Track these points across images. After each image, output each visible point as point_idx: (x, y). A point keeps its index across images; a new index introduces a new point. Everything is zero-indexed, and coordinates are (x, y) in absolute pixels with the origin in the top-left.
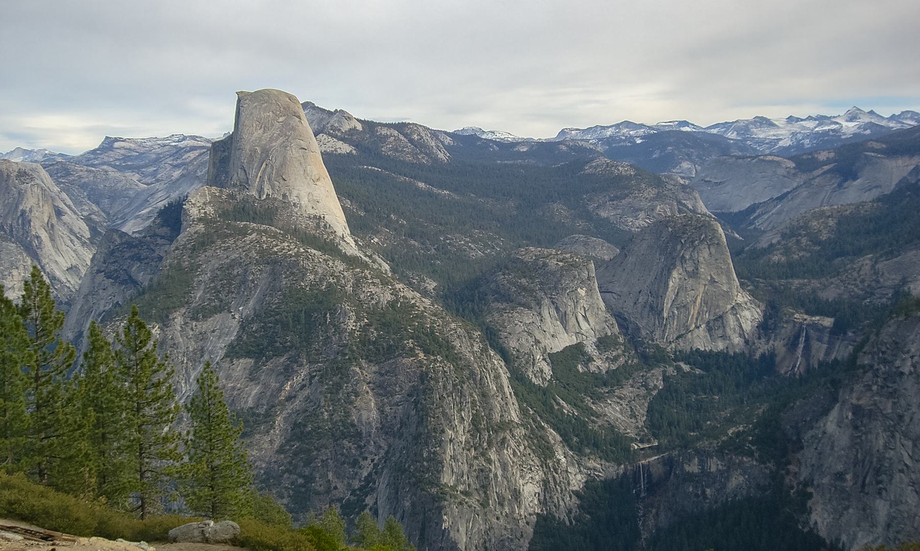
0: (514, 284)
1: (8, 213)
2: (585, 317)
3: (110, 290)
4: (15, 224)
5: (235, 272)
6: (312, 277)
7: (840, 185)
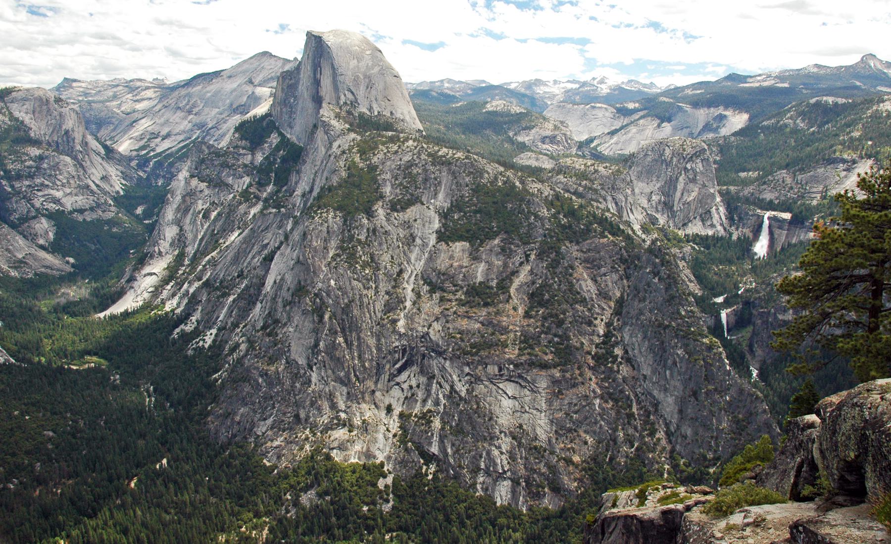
0: (580, 185)
1: (53, 132)
2: (631, 209)
3: (207, 192)
4: (60, 141)
5: (415, 171)
7: (659, 126)
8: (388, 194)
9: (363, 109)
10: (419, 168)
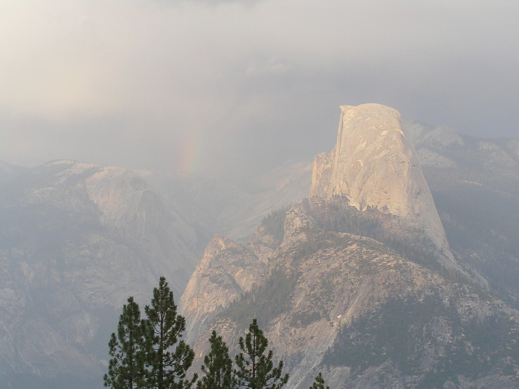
5: (335, 281)
6: (409, 289)
8: (297, 306)
9: (354, 203)
10: (341, 277)
